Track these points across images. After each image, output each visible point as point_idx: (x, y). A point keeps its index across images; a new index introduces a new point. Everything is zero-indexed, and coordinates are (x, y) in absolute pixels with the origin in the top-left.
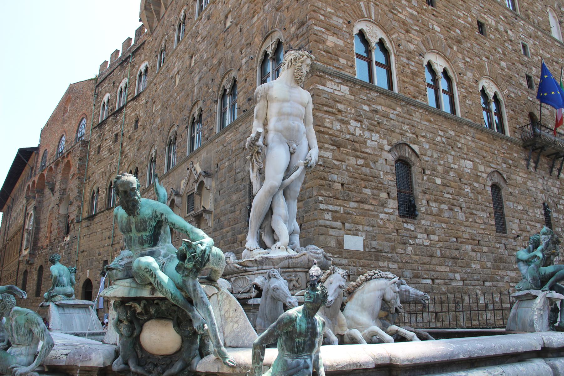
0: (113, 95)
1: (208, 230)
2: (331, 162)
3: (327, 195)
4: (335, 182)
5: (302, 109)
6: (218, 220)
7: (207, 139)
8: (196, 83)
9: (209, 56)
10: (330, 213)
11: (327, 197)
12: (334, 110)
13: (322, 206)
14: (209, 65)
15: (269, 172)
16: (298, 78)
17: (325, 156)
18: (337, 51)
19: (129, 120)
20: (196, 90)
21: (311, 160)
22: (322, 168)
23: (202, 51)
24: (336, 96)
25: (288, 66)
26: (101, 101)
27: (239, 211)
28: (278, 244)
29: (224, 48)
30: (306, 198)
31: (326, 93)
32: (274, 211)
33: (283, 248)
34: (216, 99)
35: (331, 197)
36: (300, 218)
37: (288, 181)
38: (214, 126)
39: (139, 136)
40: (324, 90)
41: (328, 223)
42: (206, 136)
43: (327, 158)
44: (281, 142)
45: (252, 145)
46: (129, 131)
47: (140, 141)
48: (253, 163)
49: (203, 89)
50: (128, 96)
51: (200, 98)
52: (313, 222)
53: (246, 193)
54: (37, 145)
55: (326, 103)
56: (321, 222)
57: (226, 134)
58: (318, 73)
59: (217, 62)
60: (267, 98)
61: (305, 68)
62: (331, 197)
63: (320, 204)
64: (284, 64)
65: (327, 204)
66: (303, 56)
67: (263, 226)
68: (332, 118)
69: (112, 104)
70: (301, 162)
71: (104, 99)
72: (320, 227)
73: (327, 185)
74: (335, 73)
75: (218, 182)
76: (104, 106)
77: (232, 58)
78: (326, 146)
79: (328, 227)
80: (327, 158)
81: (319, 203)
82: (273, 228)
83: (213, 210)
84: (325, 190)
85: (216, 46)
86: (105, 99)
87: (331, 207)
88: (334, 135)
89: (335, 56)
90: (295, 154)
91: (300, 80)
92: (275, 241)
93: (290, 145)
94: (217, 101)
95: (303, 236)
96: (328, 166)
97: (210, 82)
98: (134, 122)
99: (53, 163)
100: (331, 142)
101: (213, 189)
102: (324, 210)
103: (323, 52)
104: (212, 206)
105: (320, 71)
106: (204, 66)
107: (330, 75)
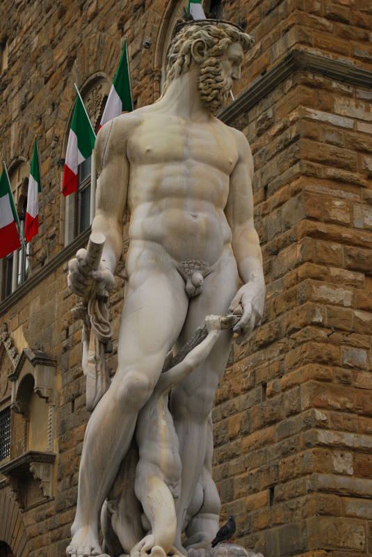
1: (45, 508)
2: (348, 314)
3: (339, 406)
4: (360, 369)
5: (223, 181)
6: (68, 480)
7: (43, 263)
8: (14, 116)
9: (45, 42)
10: (349, 455)
11: (339, 410)
12: (356, 176)
13: (324, 436)
14: (44, 67)
15: (127, 348)
16: (210, 98)
17: (332, 301)
18: (364, 16)
20: (14, 132)
21: (240, 314)
22: (323, 333)
23: (27, 30)
24: (361, 138)
25: (182, 65)
28: (149, 540)
29: (81, 19)
30: (283, 414)
32: (144, 451)
33: (158, 552)
35: (350, 411)
36: (268, 470)
37: (178, 368)
38: (57, 229)
40: (327, 123)
41: (342, 481)
42: (39, 255)
43: (338, 305)
44: (158, 267)
45: (81, 278)
48: (88, 326)
49: (31, 129)
51: (25, 154)
52: (301, 480)
55: (334, 158)
56: (324, 479)
58: (310, 77)
59: (63, 57)
60: (127, 155)
61: (227, 70)
62: (350, 411)
63: (320, 431)
64: (173, 60)
65: (340, 429)
66: (219, 36)
67: (117, 492)
68: (351, 196)
70: (214, 318)
72: (321, 495)
73: (338, 378)
74: (357, 76)
75: (70, 377)
77: (101, 44)
78: (335, 271)
79: (344, 492)
80: (338, 305)
81: (317, 427)
82: (138, 495)
83: (56, 452)
84: (335, 392)
85: (62, 14)
87: (349, 439)
88: (357, 242)
89: (362, 30)
90: (201, 299)
91: (216, 102)
92: (144, 532)
93: (185, 275)
95: (279, 520)
96: (341, 326)
97: (49, 111)
100: (349, 262)
101: (56, 394)
102: (331, 447)
103: (324, 21)
104: (55, 442)
105: (315, 71)
106: (32, 70)
107: (343, 80)
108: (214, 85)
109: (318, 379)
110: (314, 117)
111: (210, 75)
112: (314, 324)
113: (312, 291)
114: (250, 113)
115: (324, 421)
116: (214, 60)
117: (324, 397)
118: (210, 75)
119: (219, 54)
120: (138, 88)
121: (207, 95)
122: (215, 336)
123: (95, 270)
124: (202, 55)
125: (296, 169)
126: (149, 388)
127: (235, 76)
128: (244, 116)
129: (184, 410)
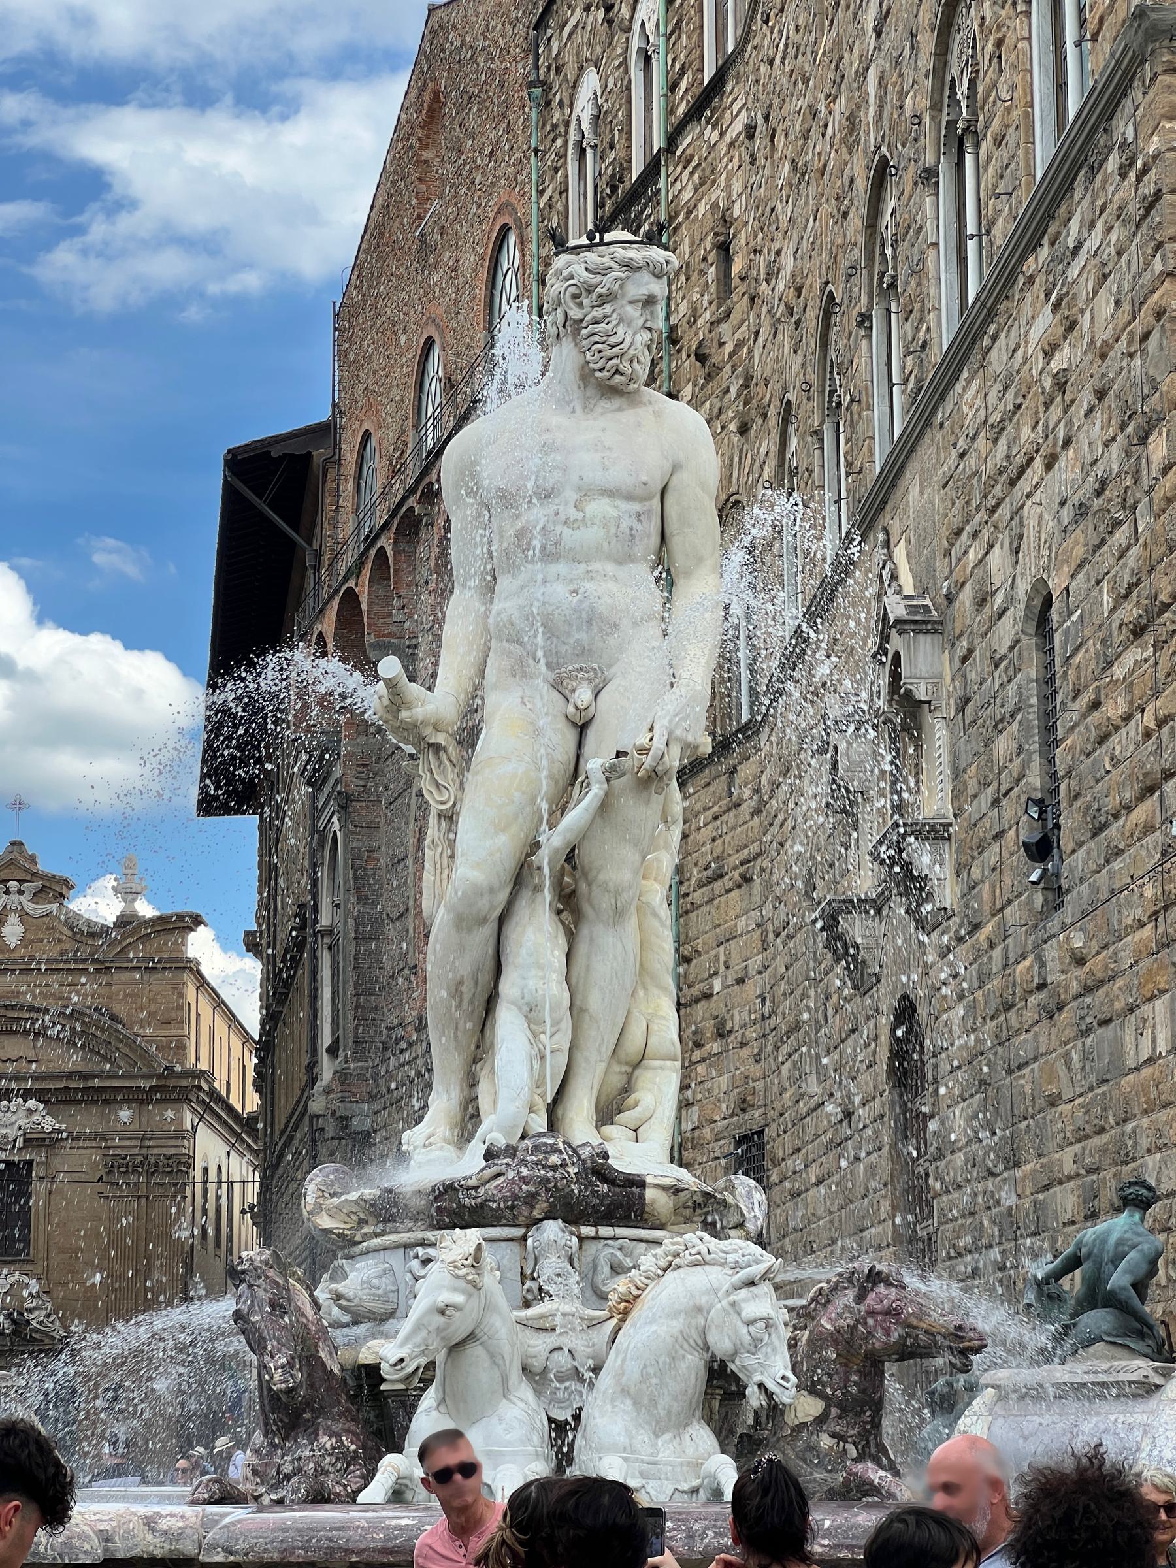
0: (610, 85)
19: (692, 244)
26: (567, 124)
27: (1012, 833)
34: (929, 159)
38: (928, 329)
39: (739, 345)
46: (695, 316)
47: (748, 378)
50: (673, 87)
53: (1029, 728)
54: (324, 415)
57: (962, 382)
69: (612, 147)
71: (577, 109)
76: (582, 152)
86: (584, 110)
91: (618, 378)
93: (567, 692)
94: (929, 176)
98: (711, 258)
99: (386, 526)
111: (596, 338)
114: (1114, 122)
118: (596, 338)
119: (607, 298)
120: (999, 28)
121: (601, 370)
122: (596, 795)
123: (409, 708)
124: (580, 305)
125: (1158, 266)
126: (492, 890)
127: (649, 324)
128: (1105, 130)
129: (586, 908)
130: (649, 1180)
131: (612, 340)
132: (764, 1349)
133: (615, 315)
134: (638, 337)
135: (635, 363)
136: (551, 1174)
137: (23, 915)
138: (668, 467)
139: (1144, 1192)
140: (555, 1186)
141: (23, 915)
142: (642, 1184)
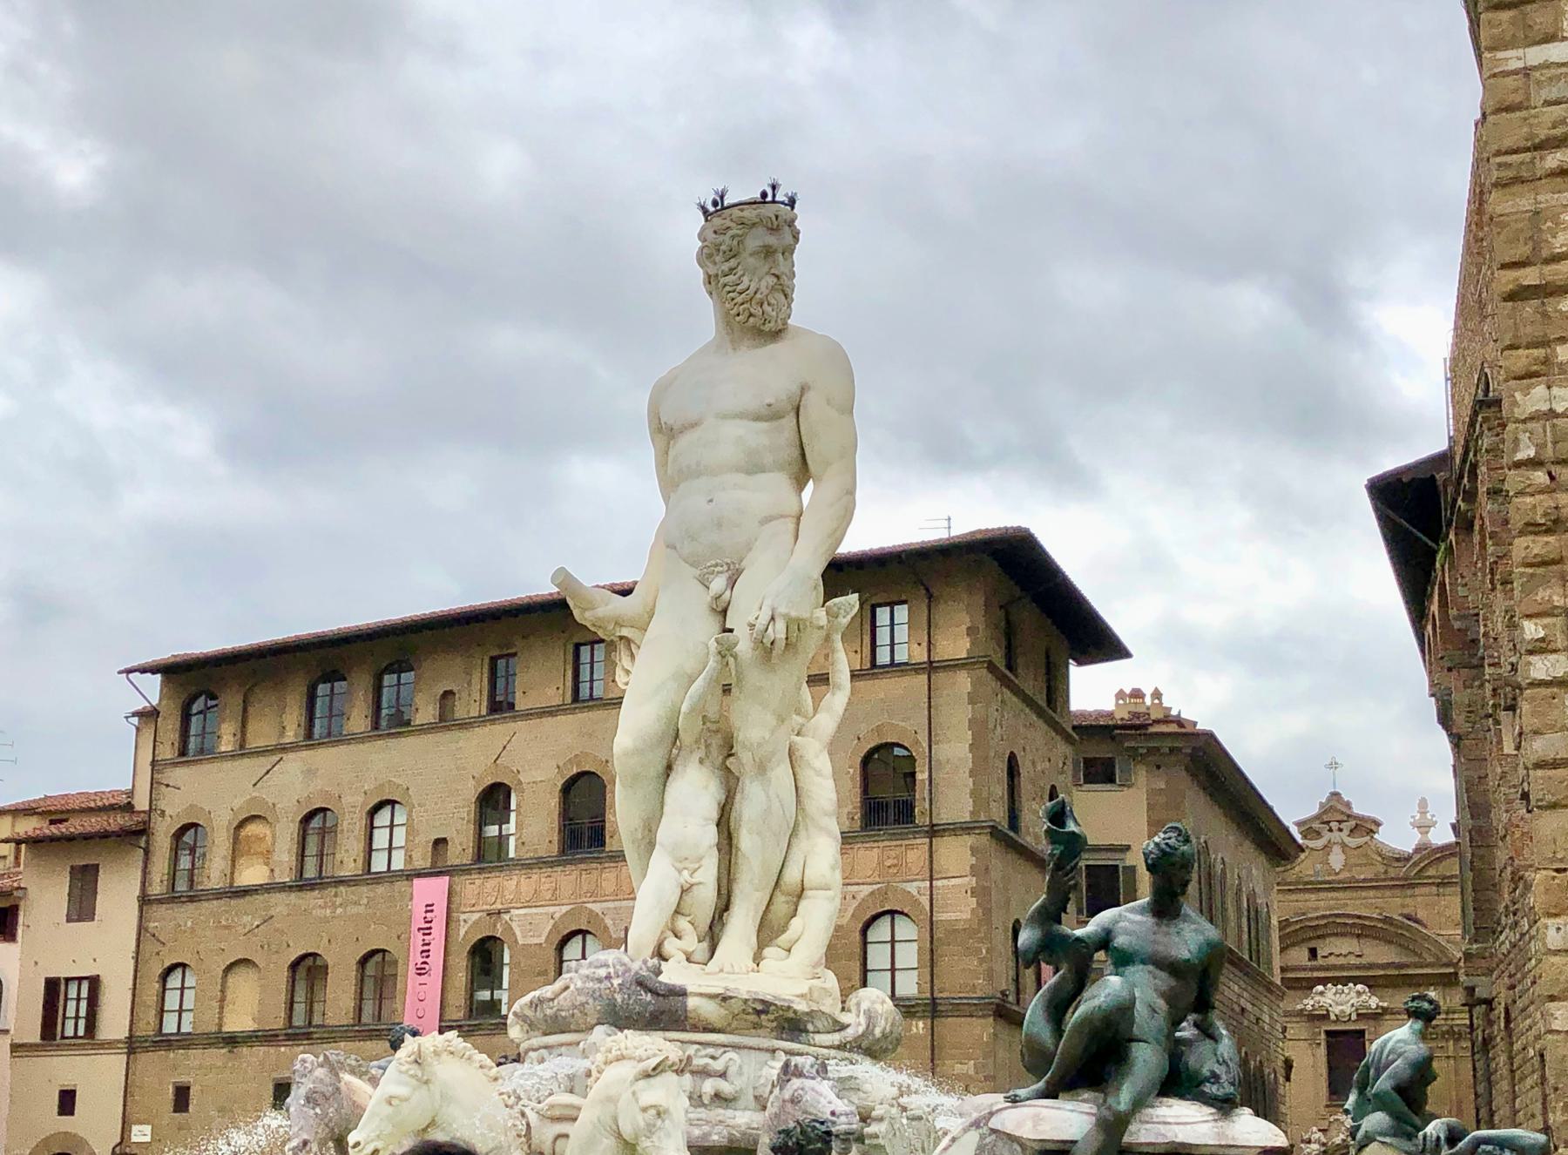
22: (1540, 477)
31: (1558, 78)
40: (1547, 65)
54: (1441, 446)
63: (1533, 659)
72: (1540, 773)
81: (1531, 652)
108: (739, 299)
109: (1531, 565)
110: (1515, 65)
111: (728, 288)
112: (1518, 465)
113: (1515, 403)
115: (1542, 640)
116: (726, 267)
117: (1542, 594)
127: (773, 271)
130: (690, 989)
131: (739, 288)
132: (657, 1134)
133: (740, 267)
134: (763, 283)
135: (765, 305)
136: (597, 986)
137: (1344, 845)
138: (795, 388)
139: (1426, 1005)
140: (600, 996)
141: (1344, 845)
142: (683, 993)
